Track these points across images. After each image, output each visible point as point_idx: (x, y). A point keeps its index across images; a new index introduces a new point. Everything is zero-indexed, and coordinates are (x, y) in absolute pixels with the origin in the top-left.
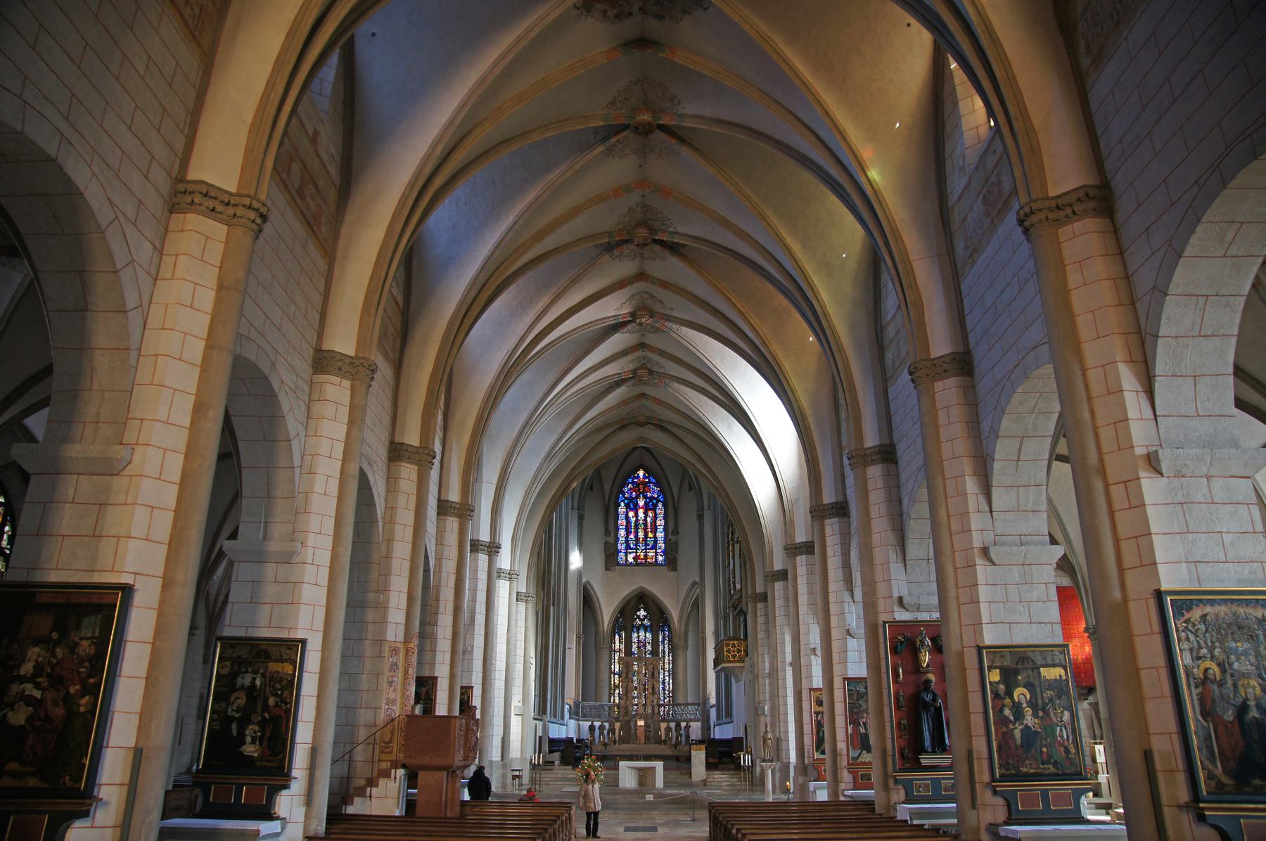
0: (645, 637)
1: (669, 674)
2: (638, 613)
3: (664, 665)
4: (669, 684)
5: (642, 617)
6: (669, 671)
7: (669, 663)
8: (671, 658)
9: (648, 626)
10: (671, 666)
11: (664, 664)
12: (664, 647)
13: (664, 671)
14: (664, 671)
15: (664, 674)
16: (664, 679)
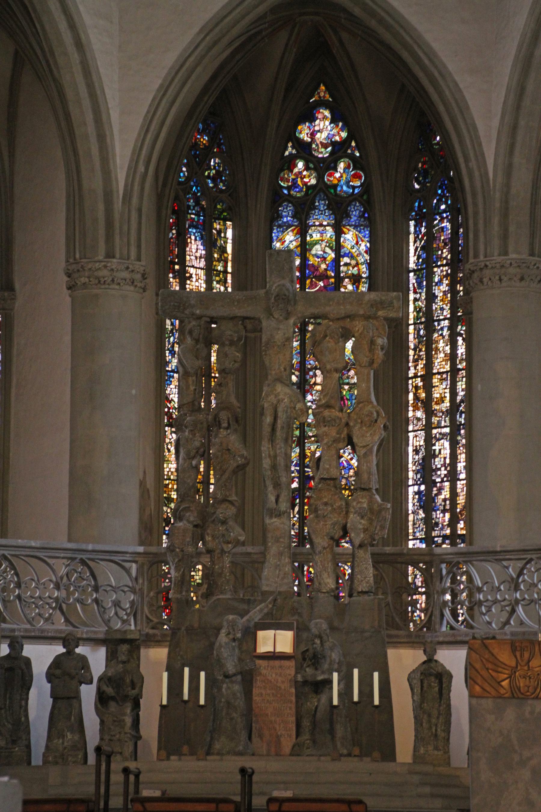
0: (338, 248)
1: (455, 428)
2: (304, 134)
3: (428, 387)
4: (453, 476)
5: (324, 153)
6: (453, 411)
7: (454, 371)
8: (461, 350)
9: (352, 198)
10: (461, 385)
11: (427, 378)
12: (431, 298)
13: (430, 413)
14: (430, 413)
15: (428, 427)
16: (430, 455)
